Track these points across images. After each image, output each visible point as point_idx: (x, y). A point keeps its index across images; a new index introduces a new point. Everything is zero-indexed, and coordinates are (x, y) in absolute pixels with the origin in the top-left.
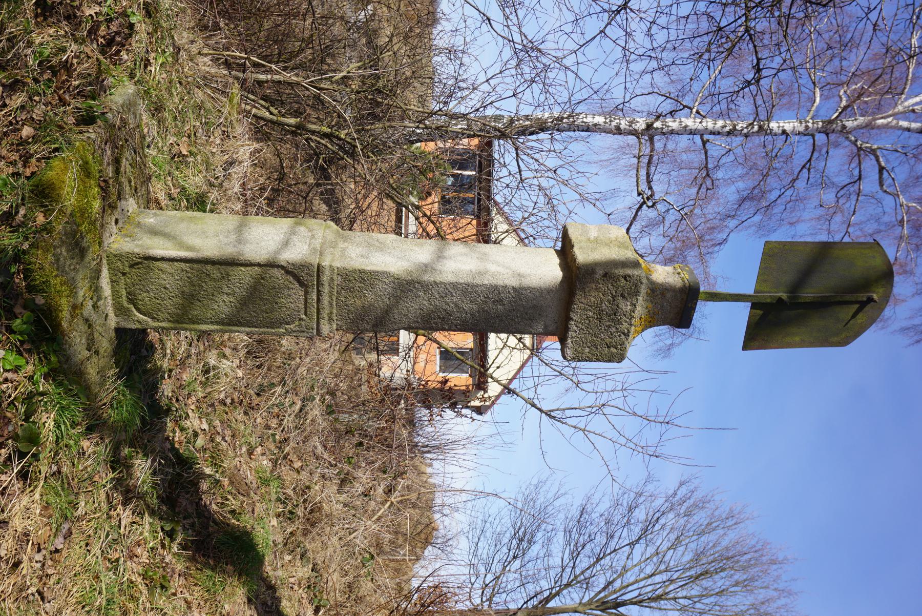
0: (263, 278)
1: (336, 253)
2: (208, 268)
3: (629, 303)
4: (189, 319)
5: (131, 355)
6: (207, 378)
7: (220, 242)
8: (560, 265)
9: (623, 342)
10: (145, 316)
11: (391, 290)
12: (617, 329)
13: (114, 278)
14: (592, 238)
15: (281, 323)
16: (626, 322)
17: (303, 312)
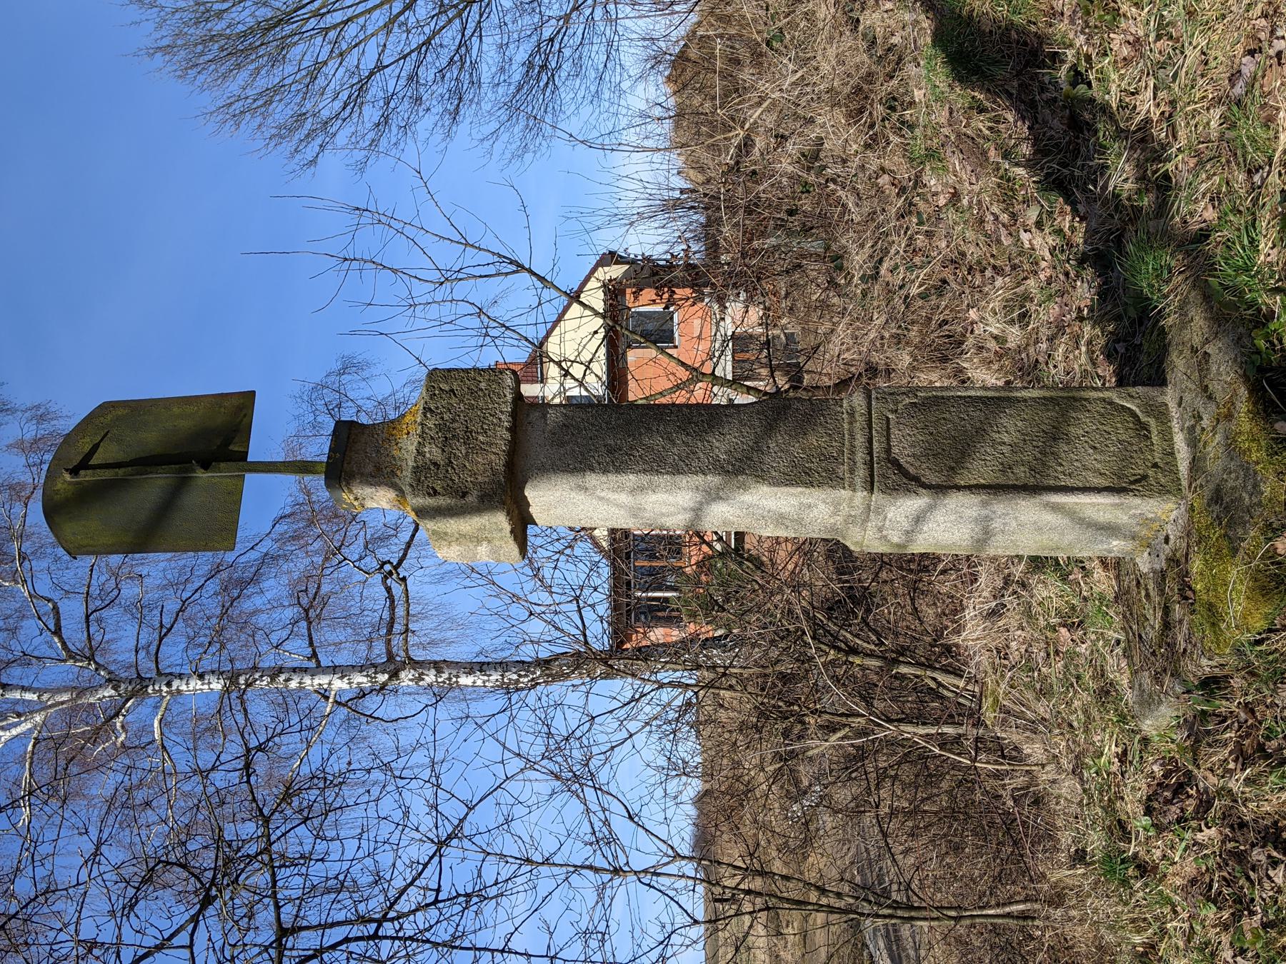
0: (952, 468)
1: (847, 509)
2: (1032, 480)
3: (428, 455)
4: (1058, 405)
5: (1141, 344)
6: (1022, 306)
7: (1016, 518)
8: (528, 505)
9: (431, 399)
10: (1122, 406)
11: (767, 459)
12: (442, 418)
13: (1170, 459)
14: (485, 544)
15: (923, 404)
16: (430, 429)
17: (892, 422)
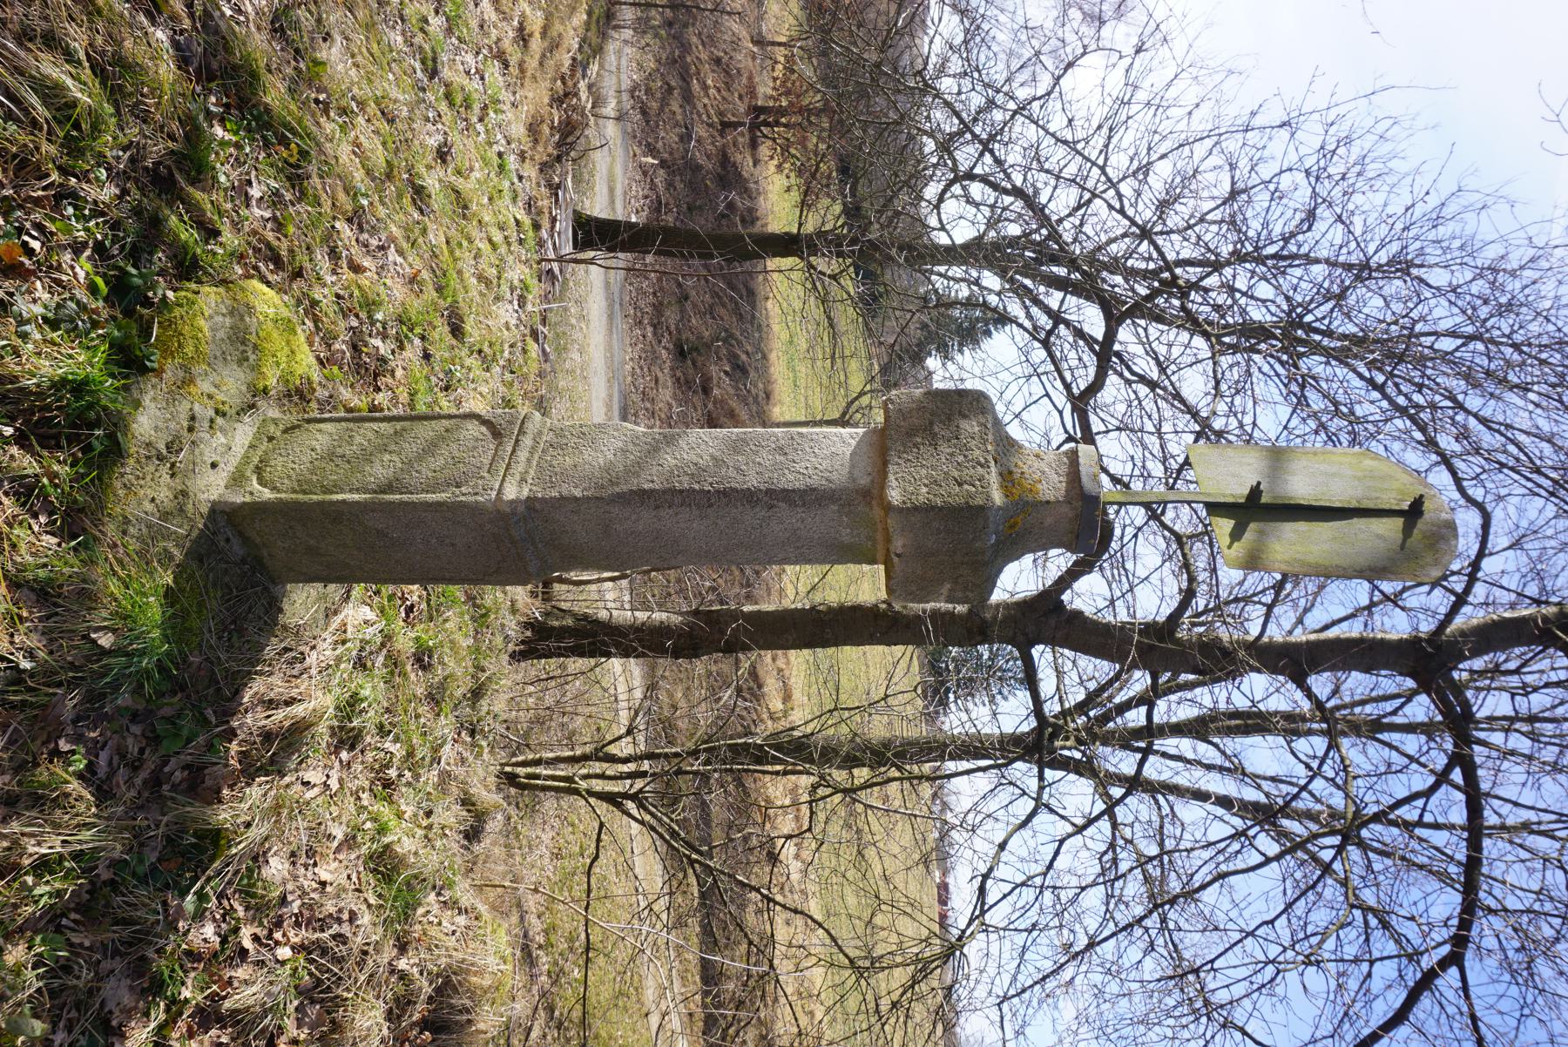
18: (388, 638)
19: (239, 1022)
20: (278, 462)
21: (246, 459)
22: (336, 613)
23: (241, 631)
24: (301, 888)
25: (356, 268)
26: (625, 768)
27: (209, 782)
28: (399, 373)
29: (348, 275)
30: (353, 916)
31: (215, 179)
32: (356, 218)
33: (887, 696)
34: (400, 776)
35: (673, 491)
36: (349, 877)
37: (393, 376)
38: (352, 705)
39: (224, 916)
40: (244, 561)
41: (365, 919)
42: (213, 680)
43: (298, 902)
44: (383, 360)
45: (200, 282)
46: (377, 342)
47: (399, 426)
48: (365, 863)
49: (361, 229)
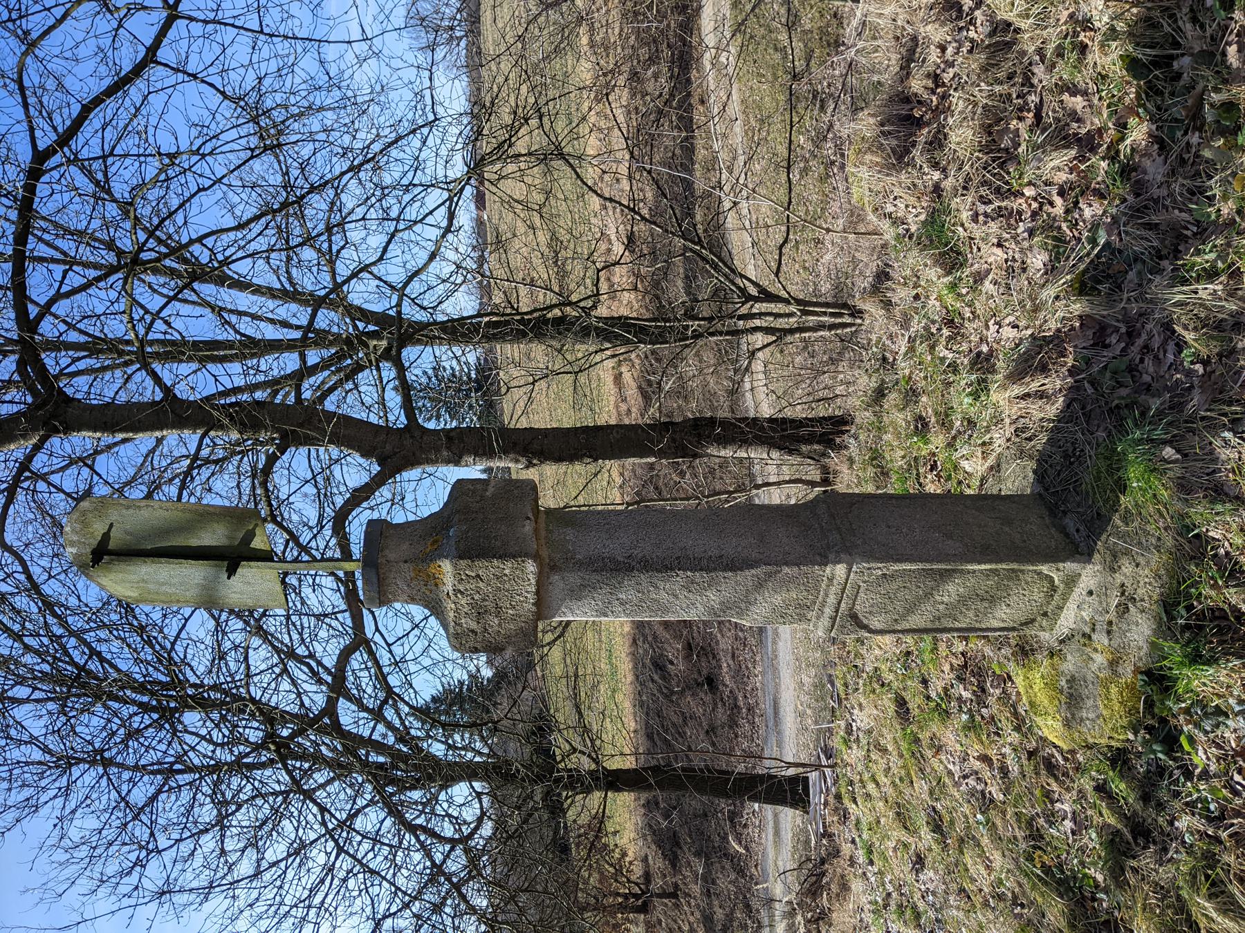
11: (752, 608)
18: (951, 445)
19: (1064, 138)
20: (1038, 596)
21: (1065, 598)
22: (991, 468)
23: (1066, 456)
24: (1017, 243)
25: (985, 758)
26: (757, 323)
27: (1090, 333)
28: (947, 668)
29: (992, 753)
30: (975, 218)
31: (1100, 835)
32: (985, 802)
33: (533, 384)
34: (939, 330)
35: (708, 570)
36: (979, 249)
37: (951, 665)
38: (979, 390)
39: (1077, 224)
40: (1065, 513)
41: (965, 215)
42: (1088, 416)
43: (1019, 231)
44: (960, 679)
45: (1110, 747)
46: (966, 695)
47: (937, 625)
48: (966, 260)
49: (983, 792)
